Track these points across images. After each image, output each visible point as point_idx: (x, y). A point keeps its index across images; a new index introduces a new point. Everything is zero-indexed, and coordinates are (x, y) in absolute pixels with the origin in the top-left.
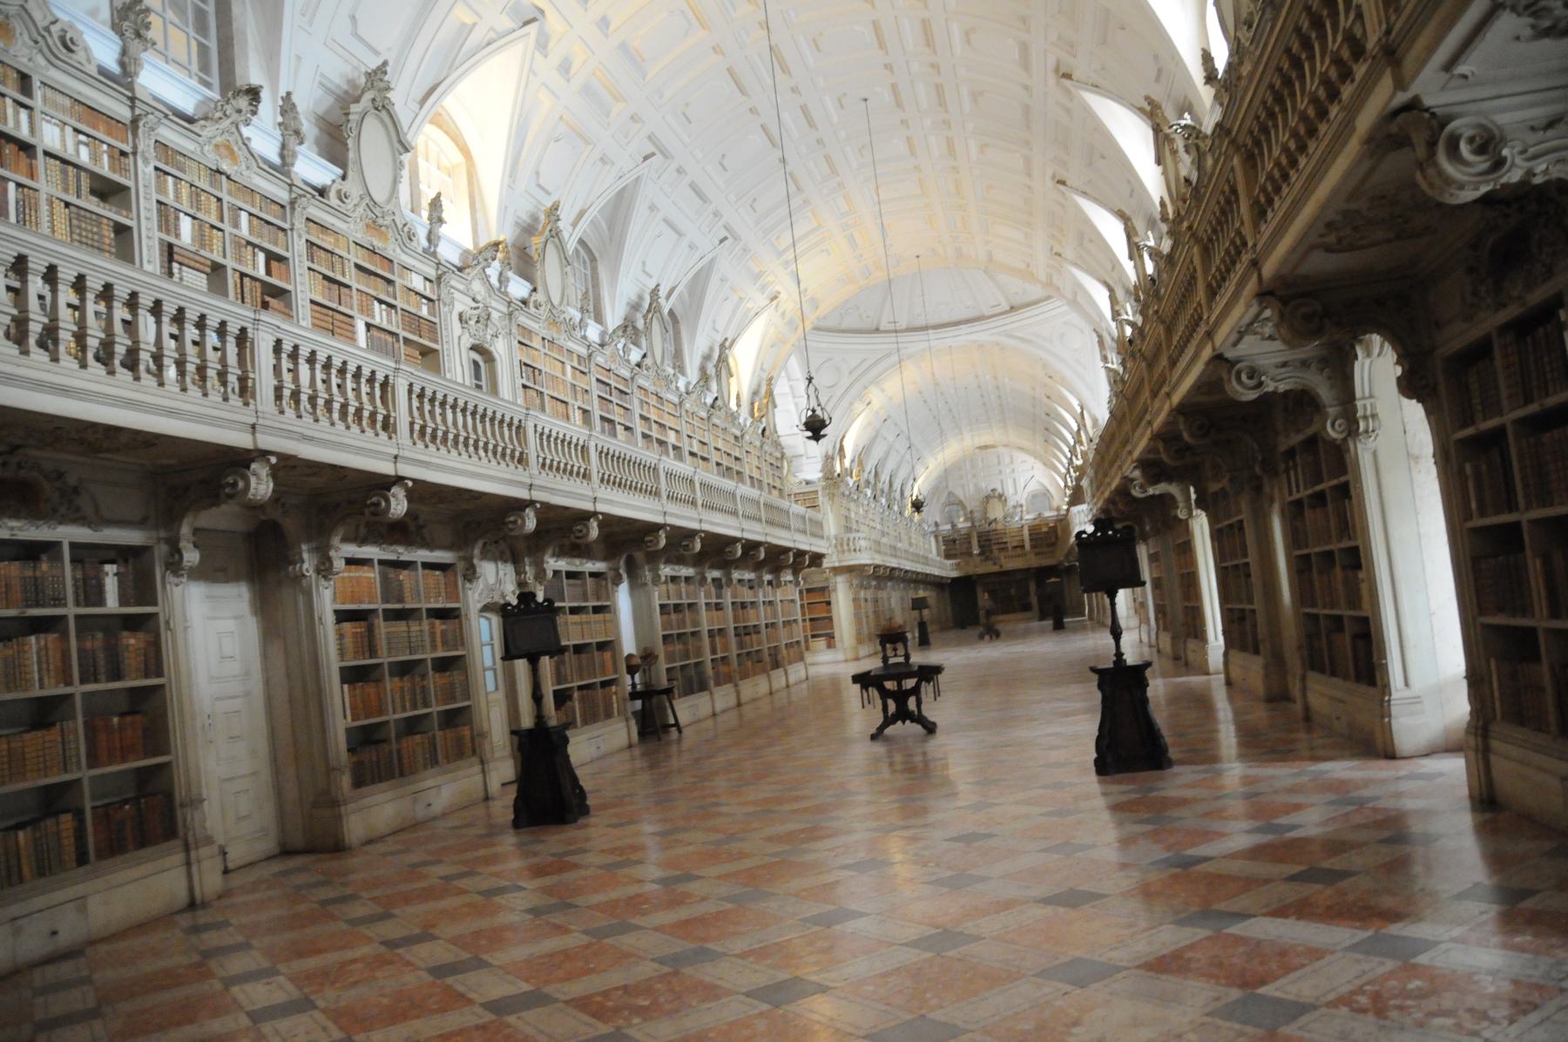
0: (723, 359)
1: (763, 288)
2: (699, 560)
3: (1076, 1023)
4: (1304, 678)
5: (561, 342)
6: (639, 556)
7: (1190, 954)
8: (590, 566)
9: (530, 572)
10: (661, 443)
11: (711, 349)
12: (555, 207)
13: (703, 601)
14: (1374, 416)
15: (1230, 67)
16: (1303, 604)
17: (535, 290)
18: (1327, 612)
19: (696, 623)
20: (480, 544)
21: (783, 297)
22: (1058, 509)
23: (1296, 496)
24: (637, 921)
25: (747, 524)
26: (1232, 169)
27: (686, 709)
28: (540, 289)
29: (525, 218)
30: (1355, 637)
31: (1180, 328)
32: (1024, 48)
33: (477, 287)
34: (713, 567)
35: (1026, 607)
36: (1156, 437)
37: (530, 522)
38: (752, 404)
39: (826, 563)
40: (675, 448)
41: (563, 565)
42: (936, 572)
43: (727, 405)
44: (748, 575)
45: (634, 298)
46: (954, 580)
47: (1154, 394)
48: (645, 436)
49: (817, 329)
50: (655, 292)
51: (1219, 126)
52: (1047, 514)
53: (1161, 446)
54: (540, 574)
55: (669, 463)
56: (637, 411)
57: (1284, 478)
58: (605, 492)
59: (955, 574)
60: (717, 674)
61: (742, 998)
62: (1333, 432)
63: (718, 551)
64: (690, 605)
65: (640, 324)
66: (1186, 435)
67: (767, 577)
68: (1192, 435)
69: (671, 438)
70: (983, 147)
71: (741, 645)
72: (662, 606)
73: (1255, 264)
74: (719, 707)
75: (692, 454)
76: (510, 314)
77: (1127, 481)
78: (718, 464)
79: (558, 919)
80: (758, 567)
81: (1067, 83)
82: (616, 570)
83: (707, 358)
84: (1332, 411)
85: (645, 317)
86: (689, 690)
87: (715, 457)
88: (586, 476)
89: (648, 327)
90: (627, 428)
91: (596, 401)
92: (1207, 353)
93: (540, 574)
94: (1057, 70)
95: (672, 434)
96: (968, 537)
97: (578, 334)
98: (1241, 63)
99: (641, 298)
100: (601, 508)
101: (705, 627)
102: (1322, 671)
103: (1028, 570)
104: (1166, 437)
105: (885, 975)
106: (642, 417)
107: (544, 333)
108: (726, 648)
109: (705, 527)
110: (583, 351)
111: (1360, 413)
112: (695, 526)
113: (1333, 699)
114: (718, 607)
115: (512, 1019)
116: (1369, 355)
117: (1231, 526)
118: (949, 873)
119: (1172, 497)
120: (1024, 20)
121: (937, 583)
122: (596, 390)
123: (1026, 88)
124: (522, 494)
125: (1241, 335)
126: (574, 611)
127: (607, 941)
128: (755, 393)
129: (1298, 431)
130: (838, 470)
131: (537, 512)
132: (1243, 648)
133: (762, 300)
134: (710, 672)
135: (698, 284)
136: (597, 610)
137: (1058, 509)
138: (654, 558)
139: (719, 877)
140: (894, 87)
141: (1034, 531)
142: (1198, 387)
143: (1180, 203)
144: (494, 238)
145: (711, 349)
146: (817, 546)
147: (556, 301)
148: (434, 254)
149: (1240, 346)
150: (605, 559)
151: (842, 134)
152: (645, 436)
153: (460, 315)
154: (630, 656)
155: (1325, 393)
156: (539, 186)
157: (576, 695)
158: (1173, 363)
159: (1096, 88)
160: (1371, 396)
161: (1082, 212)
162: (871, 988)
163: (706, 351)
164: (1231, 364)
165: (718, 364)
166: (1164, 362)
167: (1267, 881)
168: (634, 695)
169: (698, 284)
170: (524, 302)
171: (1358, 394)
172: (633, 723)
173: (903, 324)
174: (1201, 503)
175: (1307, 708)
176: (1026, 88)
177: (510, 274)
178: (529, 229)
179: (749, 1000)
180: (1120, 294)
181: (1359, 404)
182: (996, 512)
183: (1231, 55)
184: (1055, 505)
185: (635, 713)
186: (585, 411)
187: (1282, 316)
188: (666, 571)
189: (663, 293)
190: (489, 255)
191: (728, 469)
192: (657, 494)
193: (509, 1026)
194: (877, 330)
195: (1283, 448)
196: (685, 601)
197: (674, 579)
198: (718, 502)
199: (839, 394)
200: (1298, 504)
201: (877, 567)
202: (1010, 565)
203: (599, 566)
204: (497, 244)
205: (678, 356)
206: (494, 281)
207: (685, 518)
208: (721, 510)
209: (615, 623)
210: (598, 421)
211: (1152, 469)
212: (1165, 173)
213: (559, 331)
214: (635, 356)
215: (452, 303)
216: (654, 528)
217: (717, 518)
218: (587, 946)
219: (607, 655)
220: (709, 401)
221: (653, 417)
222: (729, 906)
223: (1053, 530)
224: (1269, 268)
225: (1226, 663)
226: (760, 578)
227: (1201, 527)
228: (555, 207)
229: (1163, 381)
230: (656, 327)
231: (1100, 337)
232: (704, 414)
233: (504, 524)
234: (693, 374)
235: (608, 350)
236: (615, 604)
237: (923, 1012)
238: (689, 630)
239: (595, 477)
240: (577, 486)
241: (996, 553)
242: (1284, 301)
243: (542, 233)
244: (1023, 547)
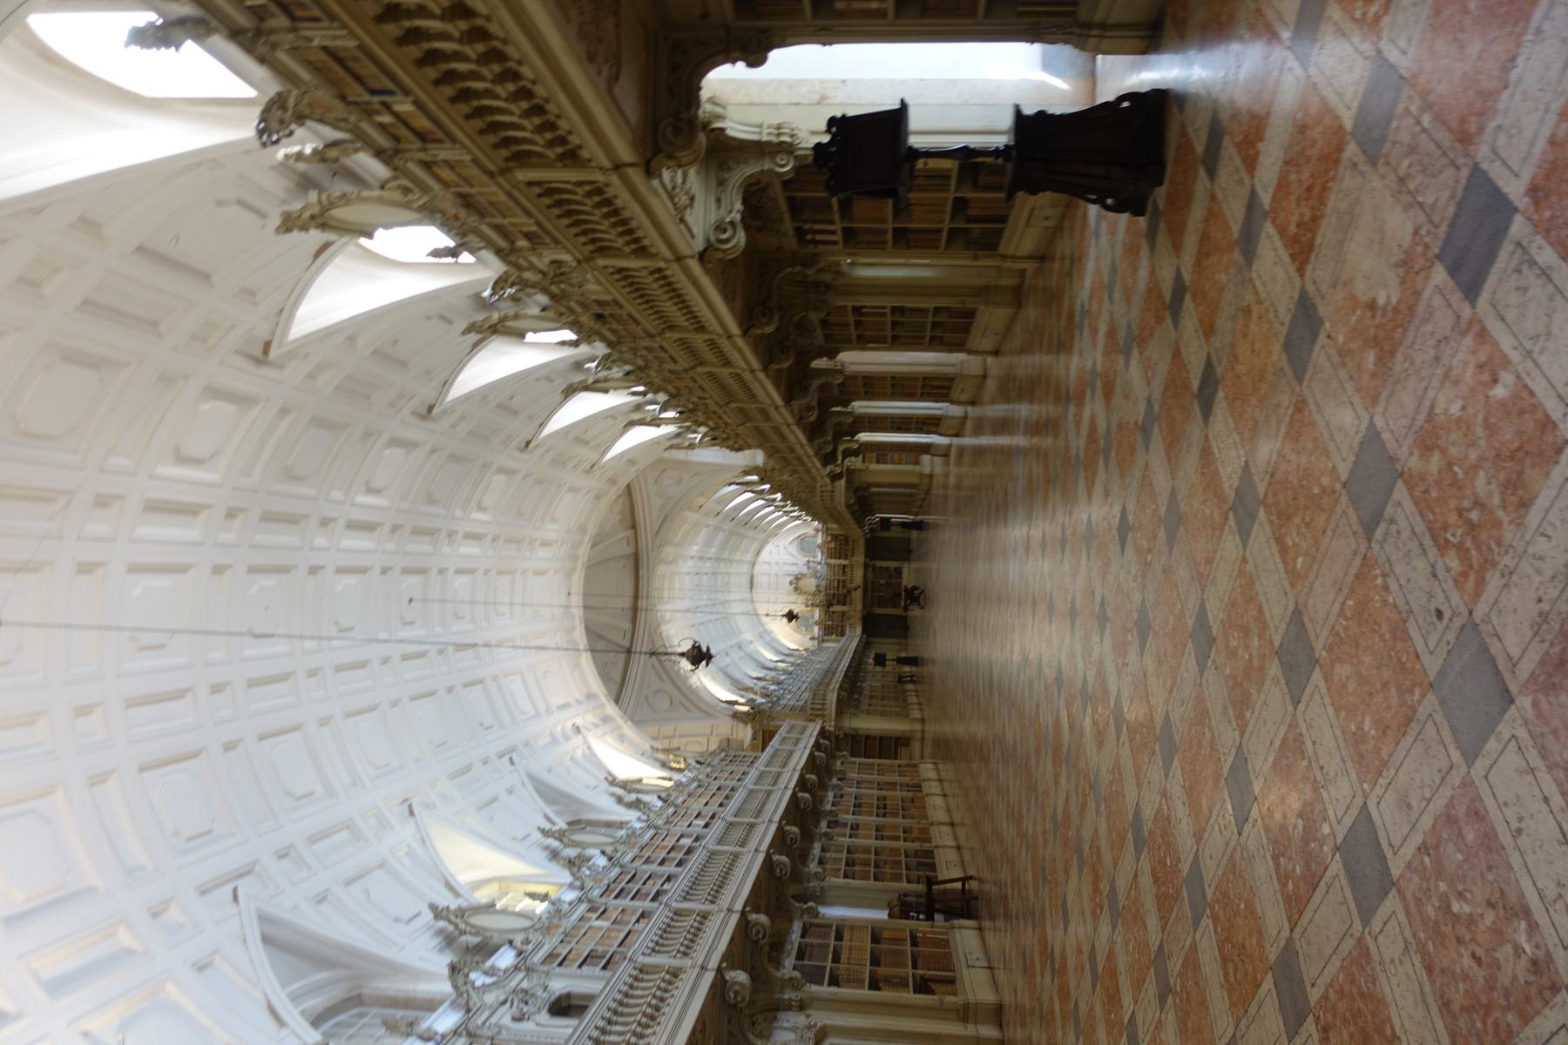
0: (625, 785)
1: (567, 738)
2: (808, 836)
3: (1372, 306)
4: (1005, 257)
5: (569, 926)
6: (793, 889)
7: (1293, 228)
8: (795, 936)
9: (788, 995)
10: (690, 851)
11: (612, 794)
12: (433, 907)
13: (847, 840)
14: (779, 127)
15: (447, 225)
16: (937, 248)
17: (511, 943)
18: (948, 216)
19: (867, 850)
20: (751, 1037)
21: (579, 721)
22: (817, 530)
23: (838, 237)
24: (1185, 867)
25: (782, 783)
26: (530, 184)
27: (949, 868)
28: (511, 937)
29: (436, 941)
30: (976, 186)
31: (670, 308)
32: (395, 442)
33: (490, 998)
34: (817, 825)
35: (899, 571)
36: (765, 369)
37: (741, 976)
38: (672, 769)
39: (830, 727)
40: (697, 839)
41: (789, 961)
42: (854, 644)
43: (667, 789)
44: (830, 795)
45: (545, 854)
46: (864, 631)
47: (727, 363)
48: (680, 864)
49: (617, 701)
50: (545, 833)
51: (499, 252)
52: (819, 540)
53: (775, 367)
54: (793, 984)
55: (710, 841)
56: (654, 867)
57: (820, 247)
58: (724, 901)
59: (859, 631)
60: (918, 839)
61: (1301, 707)
62: (786, 166)
63: (803, 815)
64: (849, 852)
65: (571, 852)
66: (769, 329)
67: (835, 781)
68: (768, 323)
69: (686, 842)
70: (481, 508)
71: (895, 815)
72: (846, 876)
73: (618, 167)
74: (953, 843)
75: (706, 826)
76: (528, 970)
77: (800, 421)
78: (721, 805)
79: (1175, 965)
80: (823, 786)
81: (436, 411)
82: (803, 912)
83: (620, 800)
84: (767, 166)
85: (566, 846)
86: (932, 867)
87: (713, 808)
88: (705, 916)
89: (575, 844)
90: (669, 879)
91: (636, 903)
92: (694, 266)
93: (793, 984)
94: (422, 417)
95: (683, 841)
97: (566, 907)
98: (443, 213)
99: (547, 848)
100: (739, 906)
101: (872, 842)
102: (1001, 231)
103: (866, 566)
104: (769, 352)
105: (1283, 551)
106: (662, 863)
107: (556, 940)
108: (895, 827)
109: (777, 818)
110: (584, 906)
111: (774, 139)
112: (774, 827)
113: (1027, 225)
114: (855, 827)
115: (1314, 995)
116: (721, 117)
117: (858, 324)
118: (1162, 534)
119: (822, 388)
120: (368, 434)
121: (864, 646)
122: (625, 902)
123: (433, 451)
124: (709, 978)
125: (682, 220)
126: (836, 959)
127: (1209, 897)
128: (664, 765)
129: (781, 220)
130: (745, 709)
131: (733, 967)
132: (966, 329)
133: (577, 741)
134: (916, 845)
135: (549, 794)
136: (839, 937)
137: (817, 530)
138: (797, 876)
139: (1139, 786)
140: (406, 571)
141: (832, 553)
142: (728, 297)
143: (564, 319)
144: (446, 971)
145: (612, 794)
146: (814, 729)
147: (527, 923)
148: (443, 1036)
149: (695, 230)
150: (791, 921)
151: (438, 630)
152: (680, 864)
153: (515, 1019)
154: (890, 915)
155: (749, 170)
156: (409, 921)
157: (920, 972)
158: (701, 328)
159: (446, 384)
160: (760, 126)
161: (557, 432)
162: (1300, 560)
163: (612, 800)
164: (709, 247)
165: (629, 793)
166: (698, 340)
167: (1213, 198)
168: (930, 918)
169: (547, 793)
170: (520, 953)
171: (755, 137)
172: (957, 922)
173: (627, 625)
174: (832, 354)
175: (1029, 257)
176: (433, 451)
177: (489, 964)
178: (449, 941)
179: (1305, 698)
180: (636, 416)
181: (765, 138)
182: (810, 584)
183: (433, 224)
185: (946, 920)
186: (643, 916)
187: (671, 157)
188: (813, 867)
189: (547, 826)
190: (461, 980)
191: (727, 797)
192: (736, 856)
193: (1325, 997)
195: (794, 241)
196: (844, 855)
197: (821, 862)
198: (754, 805)
199: (676, 694)
200: (849, 235)
201: (841, 688)
202: (858, 576)
203: (797, 927)
204: (454, 969)
205: (609, 825)
206: (488, 980)
207: (764, 835)
208: (764, 804)
209: (855, 926)
210: (656, 904)
211: (794, 385)
212: (535, 331)
213: (557, 927)
214: (602, 861)
215: (500, 1028)
216: (768, 864)
217: (770, 807)
218: (1215, 917)
219: (886, 934)
220: (660, 804)
221: (663, 854)
222: (1176, 763)
223: (835, 537)
224: (625, 153)
225: (977, 352)
226: (835, 787)
227: (855, 360)
228: (433, 907)
229: (713, 345)
230: (578, 837)
231: (671, 447)
232: (671, 810)
233: (735, 1005)
234: (631, 816)
235: (589, 884)
236: (836, 919)
237: (1338, 487)
238: (872, 856)
239: (708, 907)
240: (711, 927)
242: (657, 151)
243: (456, 926)
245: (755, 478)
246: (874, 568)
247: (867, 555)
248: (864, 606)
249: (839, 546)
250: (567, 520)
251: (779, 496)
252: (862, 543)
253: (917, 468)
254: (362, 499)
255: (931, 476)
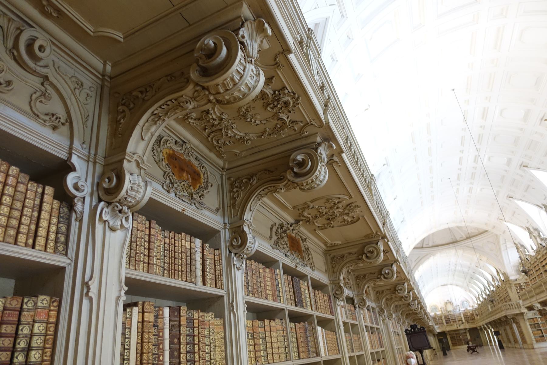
22: (473, 307)
49: (414, 248)
52: (469, 308)
81: (525, 168)
94: (521, 165)
96: (441, 317)
103: (465, 329)
120: (513, 152)
123: (506, 171)
137: (473, 307)
173: (431, 245)
176: (506, 171)
180: (532, 230)
182: (450, 308)
184: (471, 304)
194: (422, 247)
223: (472, 314)
241: (452, 323)
244: (462, 320)
245: (502, 278)
246: (466, 333)
247: (470, 329)
248: (448, 331)
249: (470, 317)
250: (477, 216)
251: (492, 288)
252: (474, 326)
253: (534, 342)
254: (486, 157)
255: (533, 348)
